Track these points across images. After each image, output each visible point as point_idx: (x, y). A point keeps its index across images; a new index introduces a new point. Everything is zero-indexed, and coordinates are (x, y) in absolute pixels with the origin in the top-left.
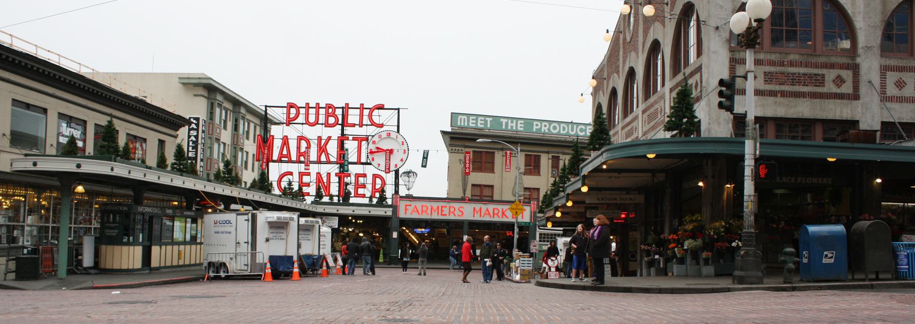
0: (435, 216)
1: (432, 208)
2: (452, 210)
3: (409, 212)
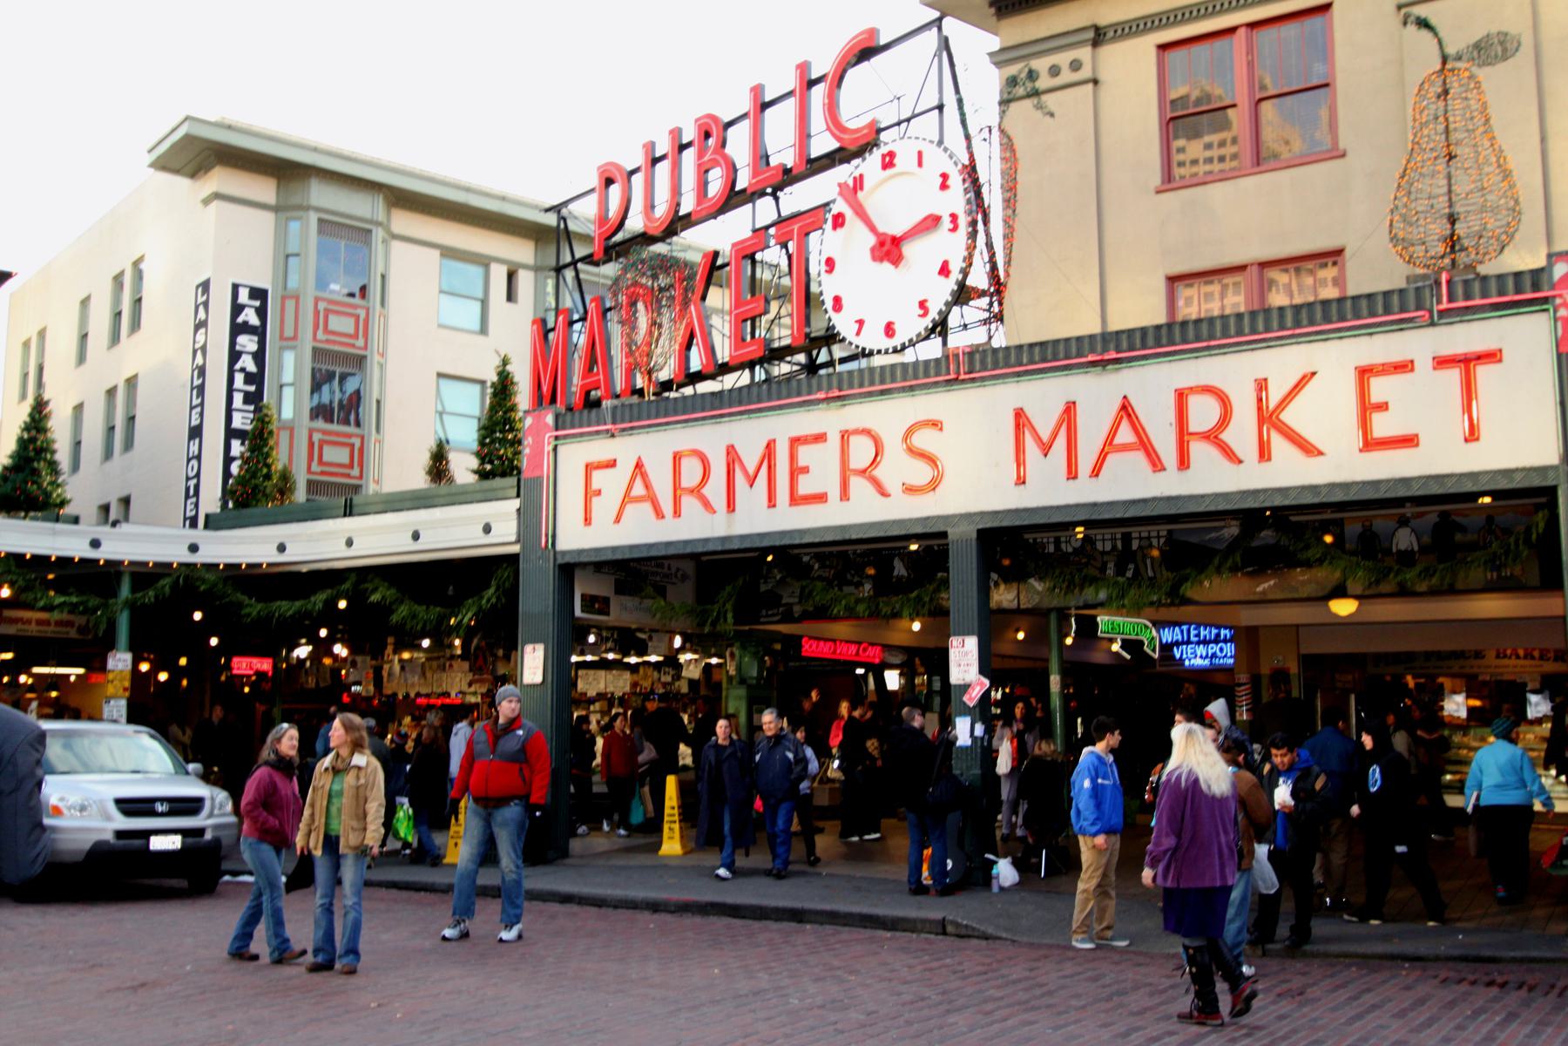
0: (757, 517)
1: (732, 456)
2: (861, 451)
3: (604, 507)
